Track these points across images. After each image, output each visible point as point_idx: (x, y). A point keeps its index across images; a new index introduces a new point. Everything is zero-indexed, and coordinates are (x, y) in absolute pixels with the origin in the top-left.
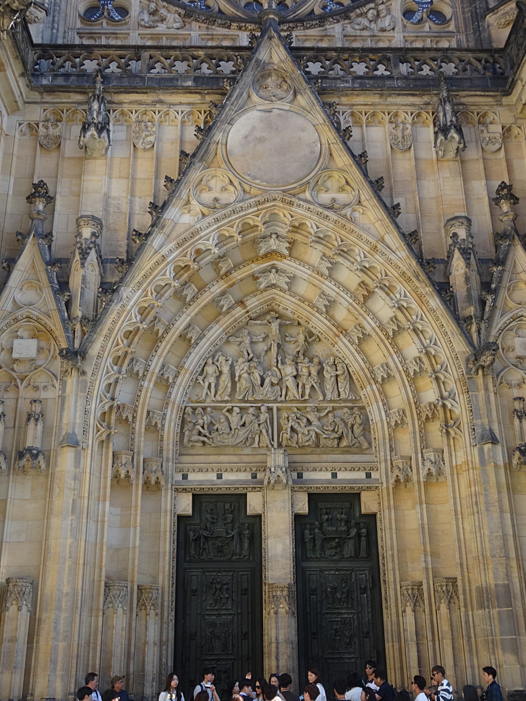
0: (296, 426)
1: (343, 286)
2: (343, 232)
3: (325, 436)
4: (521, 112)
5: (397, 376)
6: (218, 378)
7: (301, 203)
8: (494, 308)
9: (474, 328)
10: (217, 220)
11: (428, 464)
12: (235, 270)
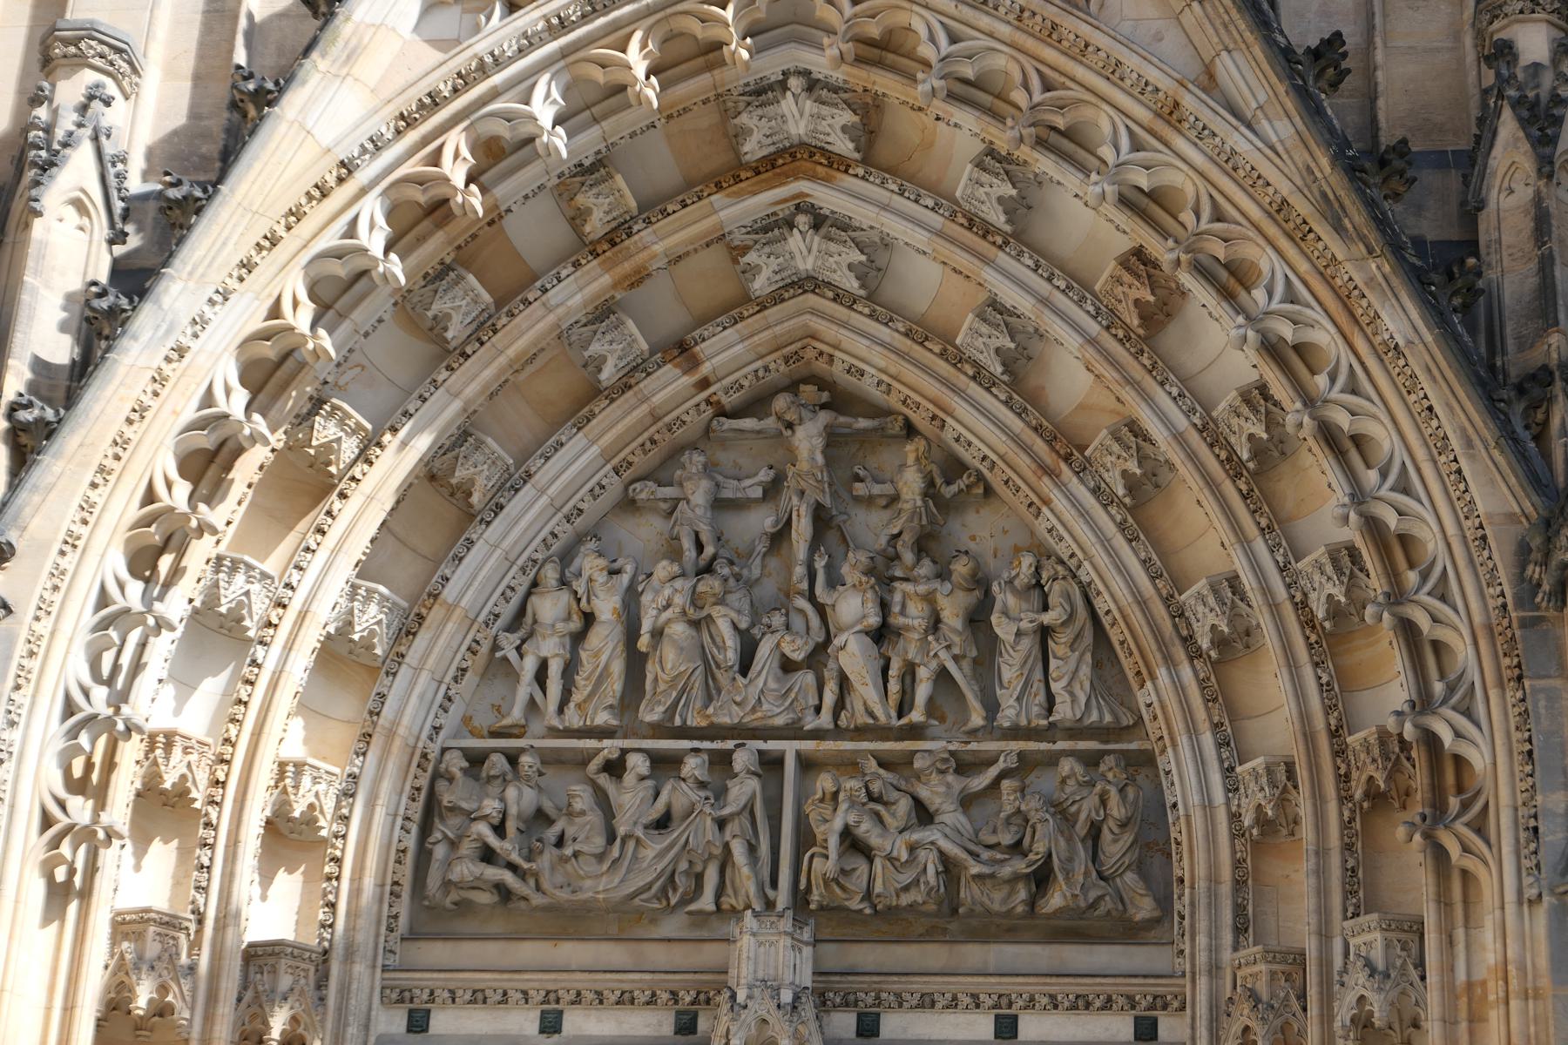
0: (866, 829)
1: (1070, 275)
2: (1050, 54)
3: (975, 869)
5: (1264, 620)
6: (578, 638)
12: (648, 222)
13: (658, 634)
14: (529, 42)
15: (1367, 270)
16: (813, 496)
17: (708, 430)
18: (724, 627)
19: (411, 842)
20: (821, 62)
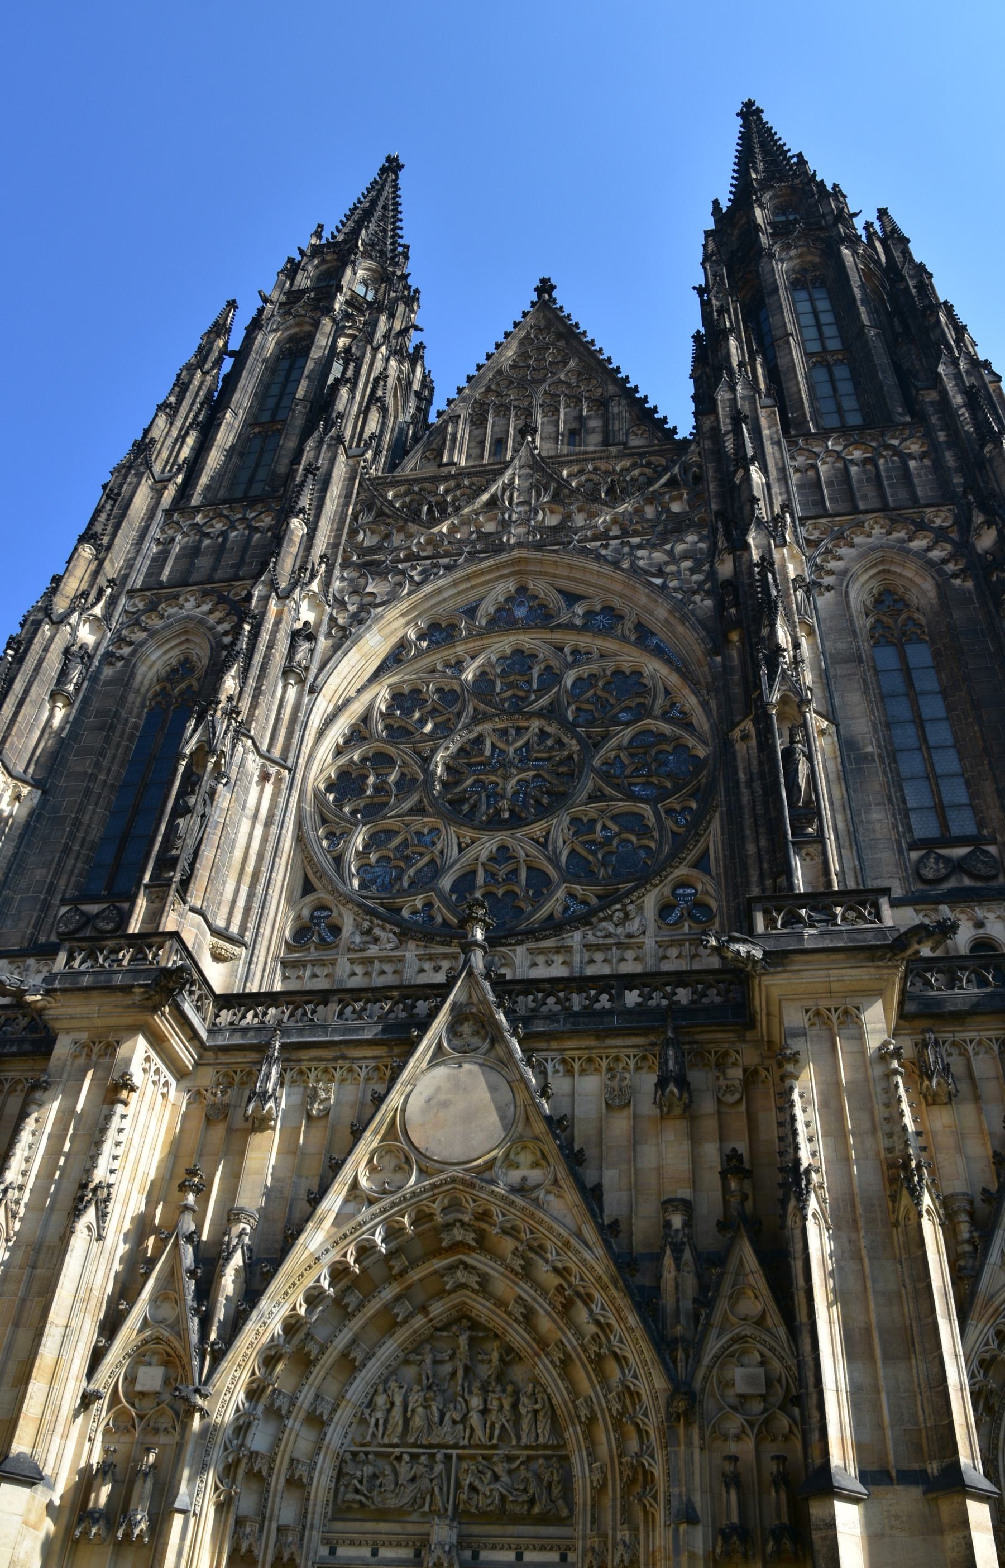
0: (477, 1483)
3: (511, 1499)
4: (769, 1049)
6: (389, 1411)
7: (484, 1184)
8: (708, 1325)
9: (680, 1355)
10: (385, 1211)
11: (621, 1547)
13: (413, 1411)
14: (375, 1216)
15: (622, 1301)
16: (464, 1361)
17: (432, 1335)
18: (434, 1408)
19: (333, 1485)
20: (466, 1218)
